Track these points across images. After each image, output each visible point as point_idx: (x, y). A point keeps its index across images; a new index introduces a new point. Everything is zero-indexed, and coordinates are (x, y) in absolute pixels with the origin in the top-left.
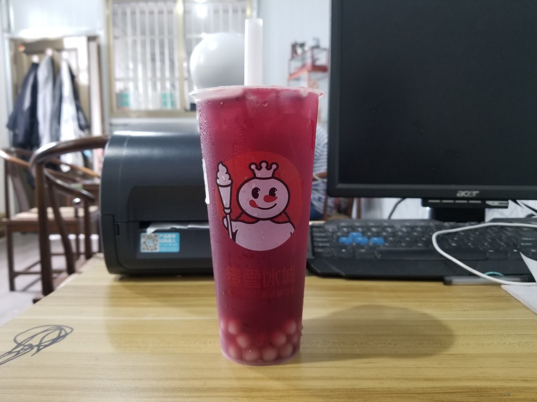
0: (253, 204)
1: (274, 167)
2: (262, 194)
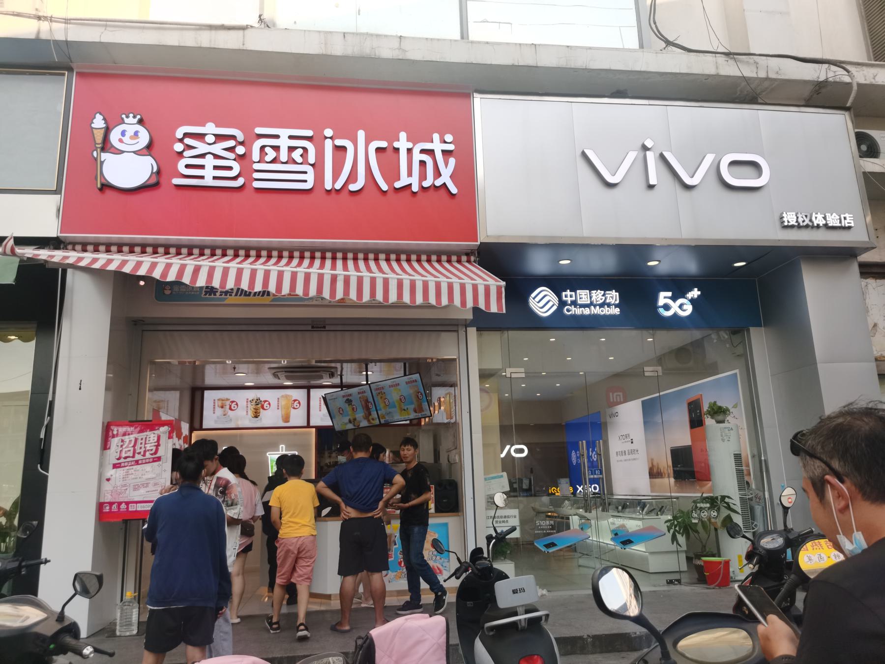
0: (121, 141)
1: (139, 117)
2: (128, 135)
